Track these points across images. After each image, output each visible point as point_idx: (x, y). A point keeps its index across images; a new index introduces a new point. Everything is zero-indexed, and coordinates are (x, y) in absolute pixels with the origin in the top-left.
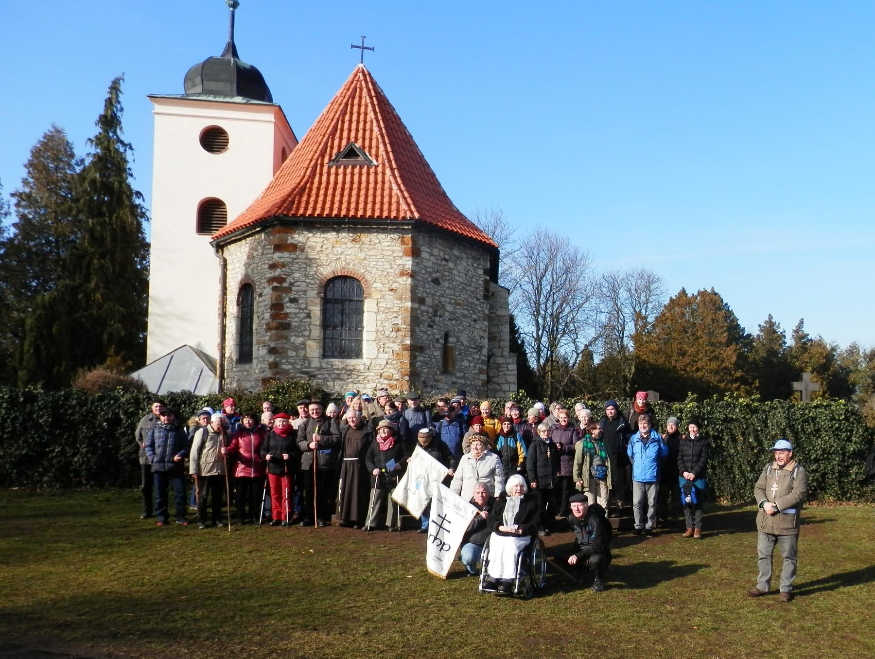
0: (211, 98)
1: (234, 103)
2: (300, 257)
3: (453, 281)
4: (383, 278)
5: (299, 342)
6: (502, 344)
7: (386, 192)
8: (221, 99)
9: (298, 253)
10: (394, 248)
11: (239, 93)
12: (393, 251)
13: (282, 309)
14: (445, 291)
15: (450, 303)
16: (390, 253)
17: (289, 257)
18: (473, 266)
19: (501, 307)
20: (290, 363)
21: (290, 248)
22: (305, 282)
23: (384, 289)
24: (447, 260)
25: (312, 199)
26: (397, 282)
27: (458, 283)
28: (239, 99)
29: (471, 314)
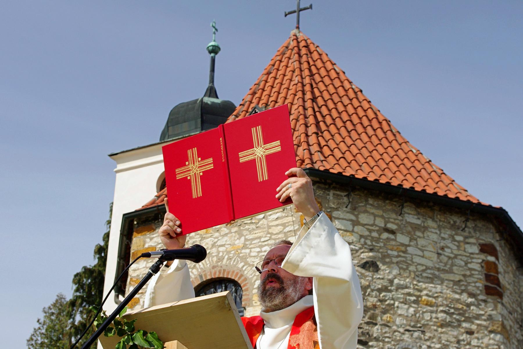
3: (408, 265)
10: (285, 220)
12: (284, 225)
14: (391, 282)
15: (405, 302)
16: (280, 228)
18: (455, 240)
24: (393, 232)
27: (421, 268)
29: (458, 321)
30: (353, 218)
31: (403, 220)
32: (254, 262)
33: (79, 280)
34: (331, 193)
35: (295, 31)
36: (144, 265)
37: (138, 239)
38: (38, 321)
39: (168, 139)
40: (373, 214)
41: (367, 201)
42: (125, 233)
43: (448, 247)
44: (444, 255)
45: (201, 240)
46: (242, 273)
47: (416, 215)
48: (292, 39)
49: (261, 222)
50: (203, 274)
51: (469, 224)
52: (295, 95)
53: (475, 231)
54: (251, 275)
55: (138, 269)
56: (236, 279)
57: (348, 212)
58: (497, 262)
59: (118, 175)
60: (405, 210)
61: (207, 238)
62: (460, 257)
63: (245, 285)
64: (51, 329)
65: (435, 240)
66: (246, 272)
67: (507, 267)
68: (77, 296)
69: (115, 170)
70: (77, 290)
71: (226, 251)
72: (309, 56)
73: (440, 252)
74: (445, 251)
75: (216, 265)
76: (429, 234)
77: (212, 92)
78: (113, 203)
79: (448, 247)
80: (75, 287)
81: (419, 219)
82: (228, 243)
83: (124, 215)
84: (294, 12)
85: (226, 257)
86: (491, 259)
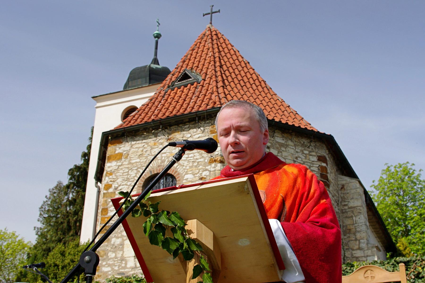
2: (124, 163)
4: (194, 169)
5: (118, 243)
6: (358, 235)
9: (123, 160)
13: (107, 213)
17: (116, 165)
18: (303, 153)
19: (352, 199)
20: (109, 265)
21: (118, 157)
22: (126, 185)
23: (195, 179)
26: (206, 170)
31: (274, 140)
32: (184, 163)
33: (72, 173)
35: (209, 25)
36: (115, 164)
37: (111, 148)
38: (46, 197)
39: (129, 88)
42: (103, 144)
43: (300, 157)
44: (297, 162)
45: (151, 150)
46: (176, 170)
47: (282, 138)
48: (208, 30)
50: (152, 170)
51: (313, 144)
52: (210, 63)
53: (315, 148)
54: (182, 171)
55: (111, 166)
56: (173, 174)
58: (327, 167)
59: (97, 109)
60: (276, 134)
61: (155, 148)
62: (306, 163)
63: (178, 177)
64: (54, 201)
65: (293, 153)
66: (179, 170)
67: (332, 170)
68: (71, 183)
69: (96, 106)
70: (71, 179)
71: (167, 156)
72: (218, 40)
73: (295, 160)
74: (298, 160)
75: (160, 165)
76: (289, 149)
77: (155, 61)
78: (93, 127)
79: (300, 157)
80: (69, 177)
81: (283, 140)
82: (168, 151)
83: (103, 133)
84: (209, 14)
85: (167, 160)
86: (324, 165)
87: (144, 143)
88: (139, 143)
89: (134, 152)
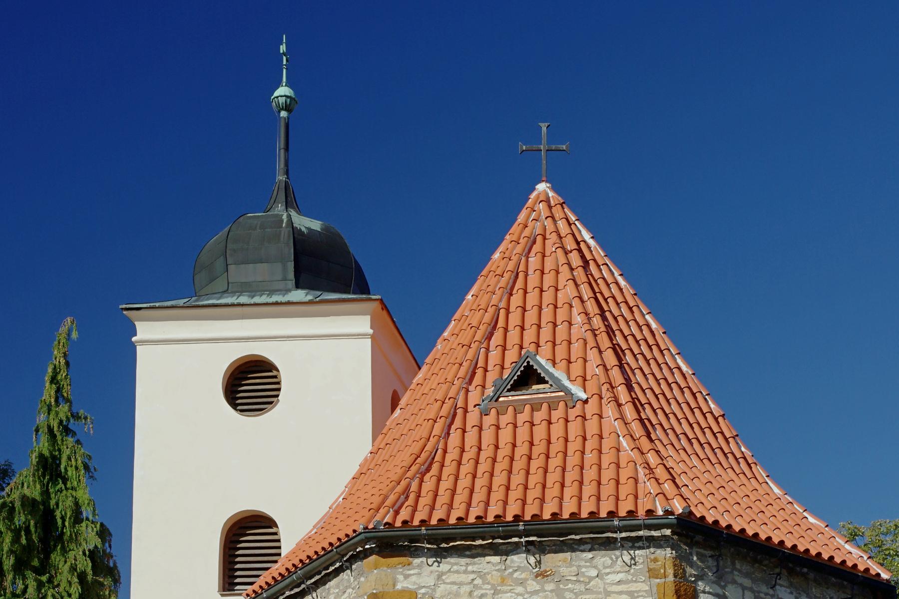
0: (244, 299)
1: (289, 303)
7: (606, 460)
8: (264, 299)
10: (633, 587)
11: (298, 286)
25: (445, 485)
28: (299, 295)
30: (720, 591)
34: (695, 550)
40: (741, 585)
41: (733, 564)
45: (493, 594)
49: (592, 583)
57: (714, 582)
61: (506, 592)
87: (473, 572)
88: (457, 572)
89: (449, 593)
